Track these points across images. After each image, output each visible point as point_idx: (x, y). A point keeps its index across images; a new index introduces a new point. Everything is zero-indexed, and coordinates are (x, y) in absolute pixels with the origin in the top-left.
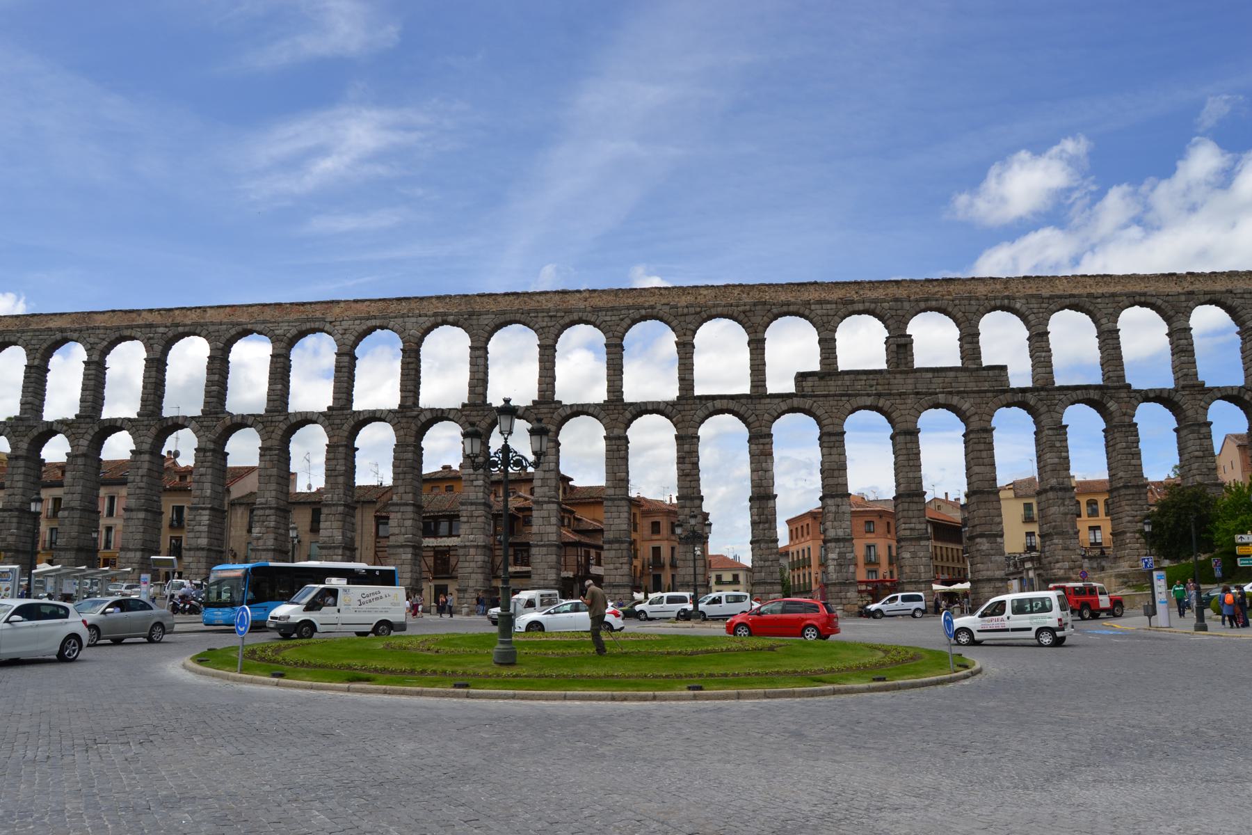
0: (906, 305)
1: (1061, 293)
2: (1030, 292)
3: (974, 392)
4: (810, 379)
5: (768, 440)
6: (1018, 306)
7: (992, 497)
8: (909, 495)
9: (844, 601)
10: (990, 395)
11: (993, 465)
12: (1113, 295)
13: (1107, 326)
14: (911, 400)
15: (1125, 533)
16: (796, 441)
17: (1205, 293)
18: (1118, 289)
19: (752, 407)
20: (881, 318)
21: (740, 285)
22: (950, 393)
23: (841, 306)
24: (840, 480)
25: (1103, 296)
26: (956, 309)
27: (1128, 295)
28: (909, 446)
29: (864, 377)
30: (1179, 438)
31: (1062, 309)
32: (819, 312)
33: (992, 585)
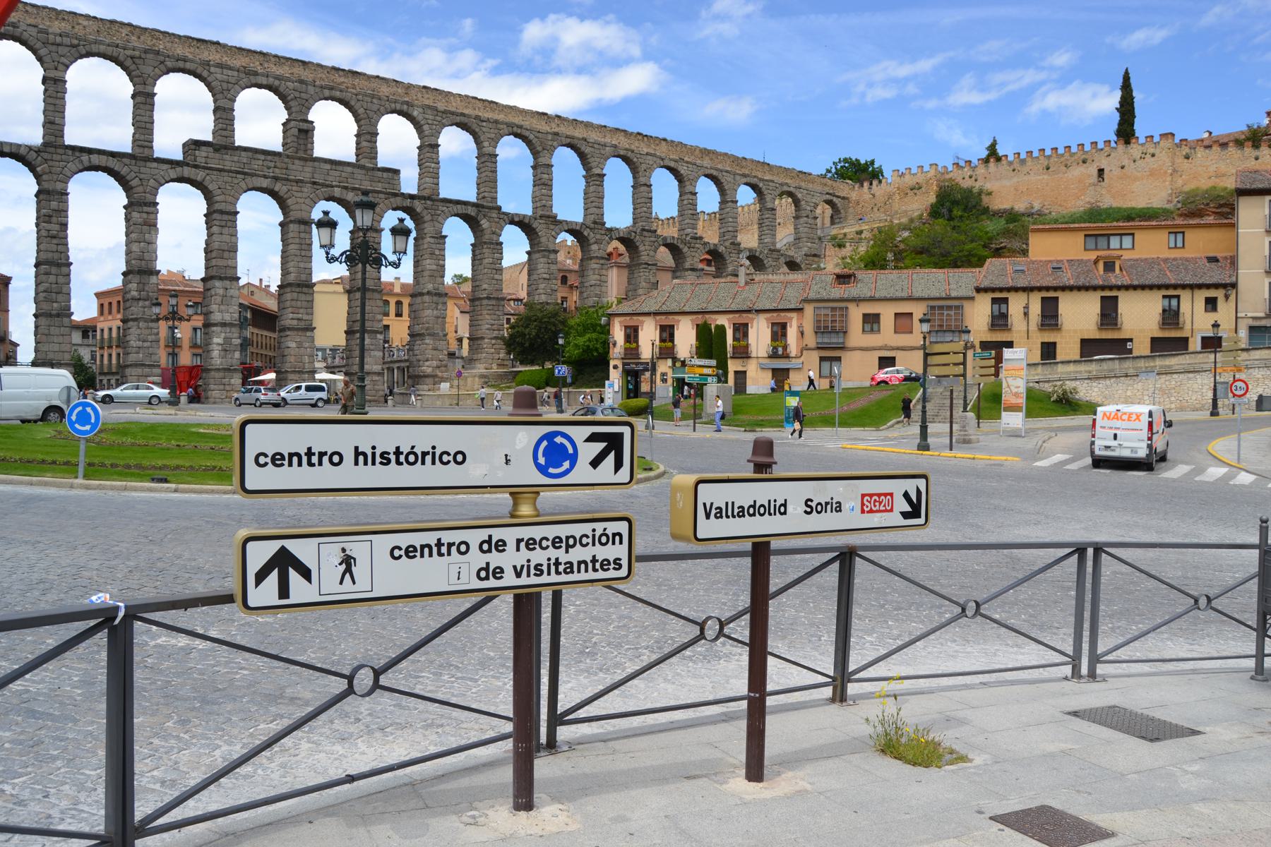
0: (311, 89)
2: (427, 102)
6: (415, 113)
8: (299, 285)
9: (228, 388)
12: (496, 122)
13: (488, 150)
14: (307, 189)
15: (483, 338)
16: (181, 213)
17: (567, 137)
18: (501, 117)
19: (136, 168)
20: (283, 97)
21: (130, 25)
22: (346, 188)
23: (243, 75)
24: (230, 263)
25: (488, 120)
26: (359, 104)
27: (509, 125)
28: (302, 235)
29: (262, 157)
32: (219, 76)
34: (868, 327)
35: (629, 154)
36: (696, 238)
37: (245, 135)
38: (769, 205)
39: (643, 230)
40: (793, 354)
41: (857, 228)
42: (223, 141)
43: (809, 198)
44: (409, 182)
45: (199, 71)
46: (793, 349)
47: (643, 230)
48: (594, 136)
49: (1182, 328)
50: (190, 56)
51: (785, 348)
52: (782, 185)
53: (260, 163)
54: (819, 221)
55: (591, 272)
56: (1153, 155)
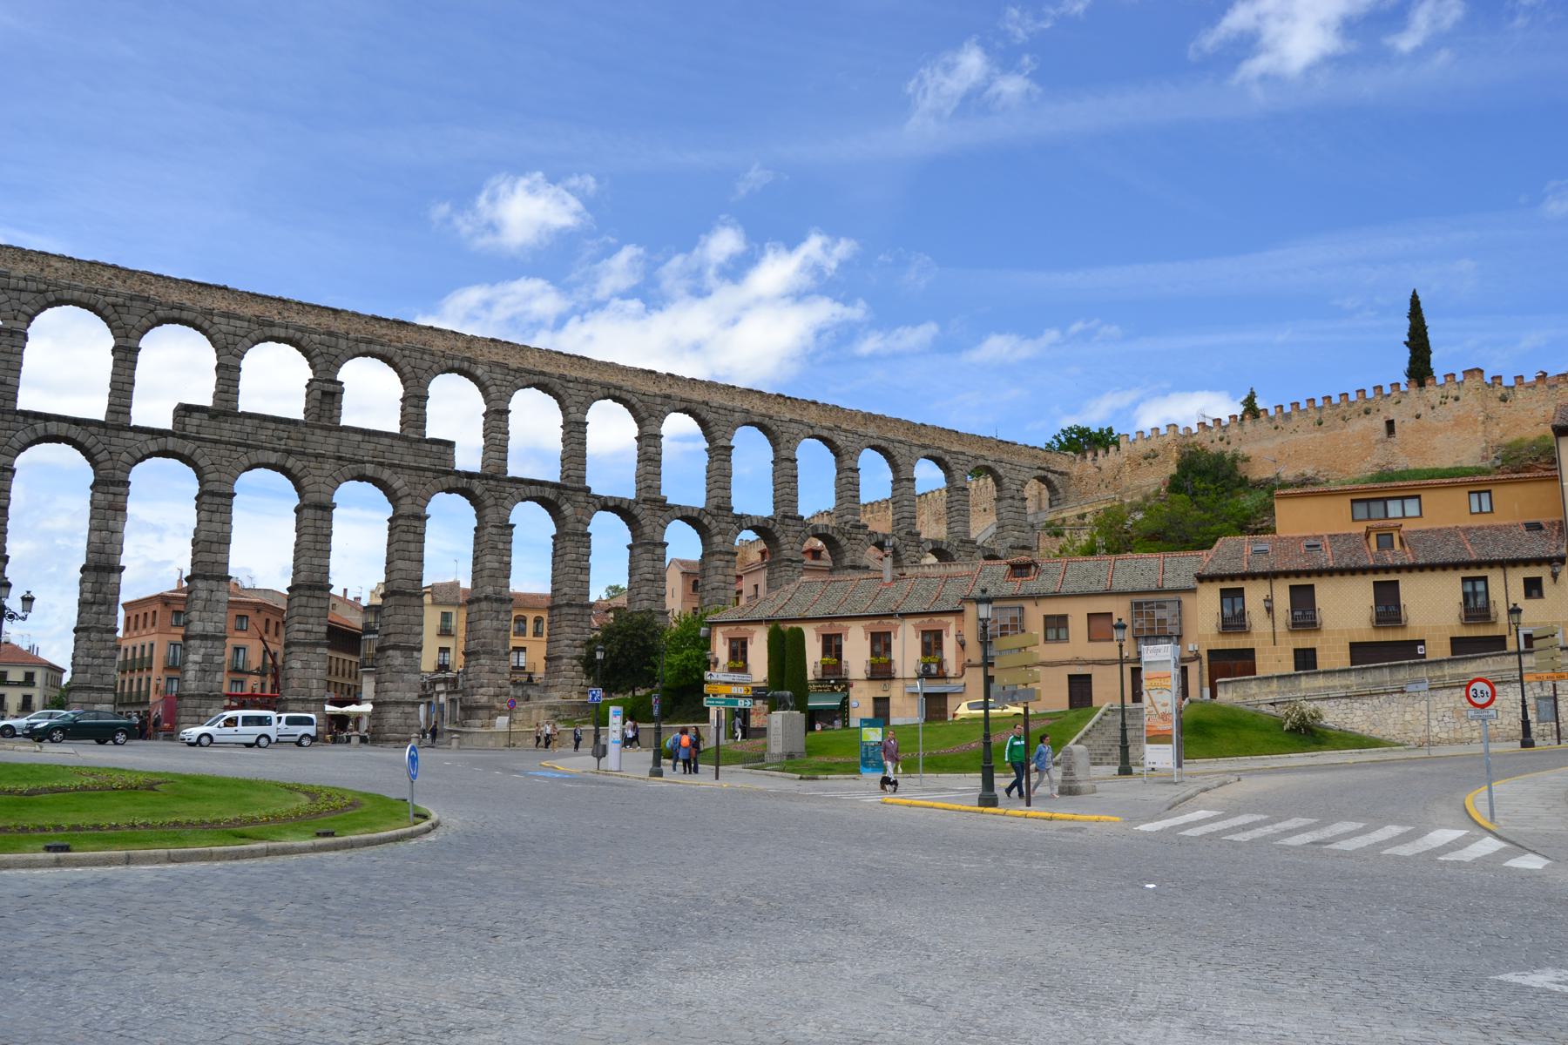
0: (343, 343)
1: (530, 367)
3: (410, 468)
4: (196, 415)
5: (122, 489)
6: (479, 372)
7: (415, 601)
8: (310, 587)
10: (430, 474)
11: (421, 561)
12: (587, 382)
14: (329, 466)
15: (560, 658)
18: (594, 376)
20: (306, 353)
21: (114, 267)
22: (381, 464)
24: (219, 557)
25: (576, 380)
26: (404, 361)
27: (603, 386)
28: (319, 523)
29: (273, 426)
30: (631, 556)
31: (528, 386)
32: (224, 328)
33: (400, 709)
34: (1052, 634)
35: (766, 421)
36: (859, 527)
37: (250, 400)
38: (959, 484)
39: (785, 517)
40: (951, 673)
41: (1079, 511)
42: (225, 405)
43: (1013, 474)
44: (468, 458)
45: (198, 322)
46: (951, 667)
47: (785, 517)
48: (717, 399)
49: (1494, 623)
50: (189, 304)
51: (940, 664)
52: (976, 457)
53: (270, 432)
54: (1028, 503)
55: (712, 572)
56: (1457, 399)
